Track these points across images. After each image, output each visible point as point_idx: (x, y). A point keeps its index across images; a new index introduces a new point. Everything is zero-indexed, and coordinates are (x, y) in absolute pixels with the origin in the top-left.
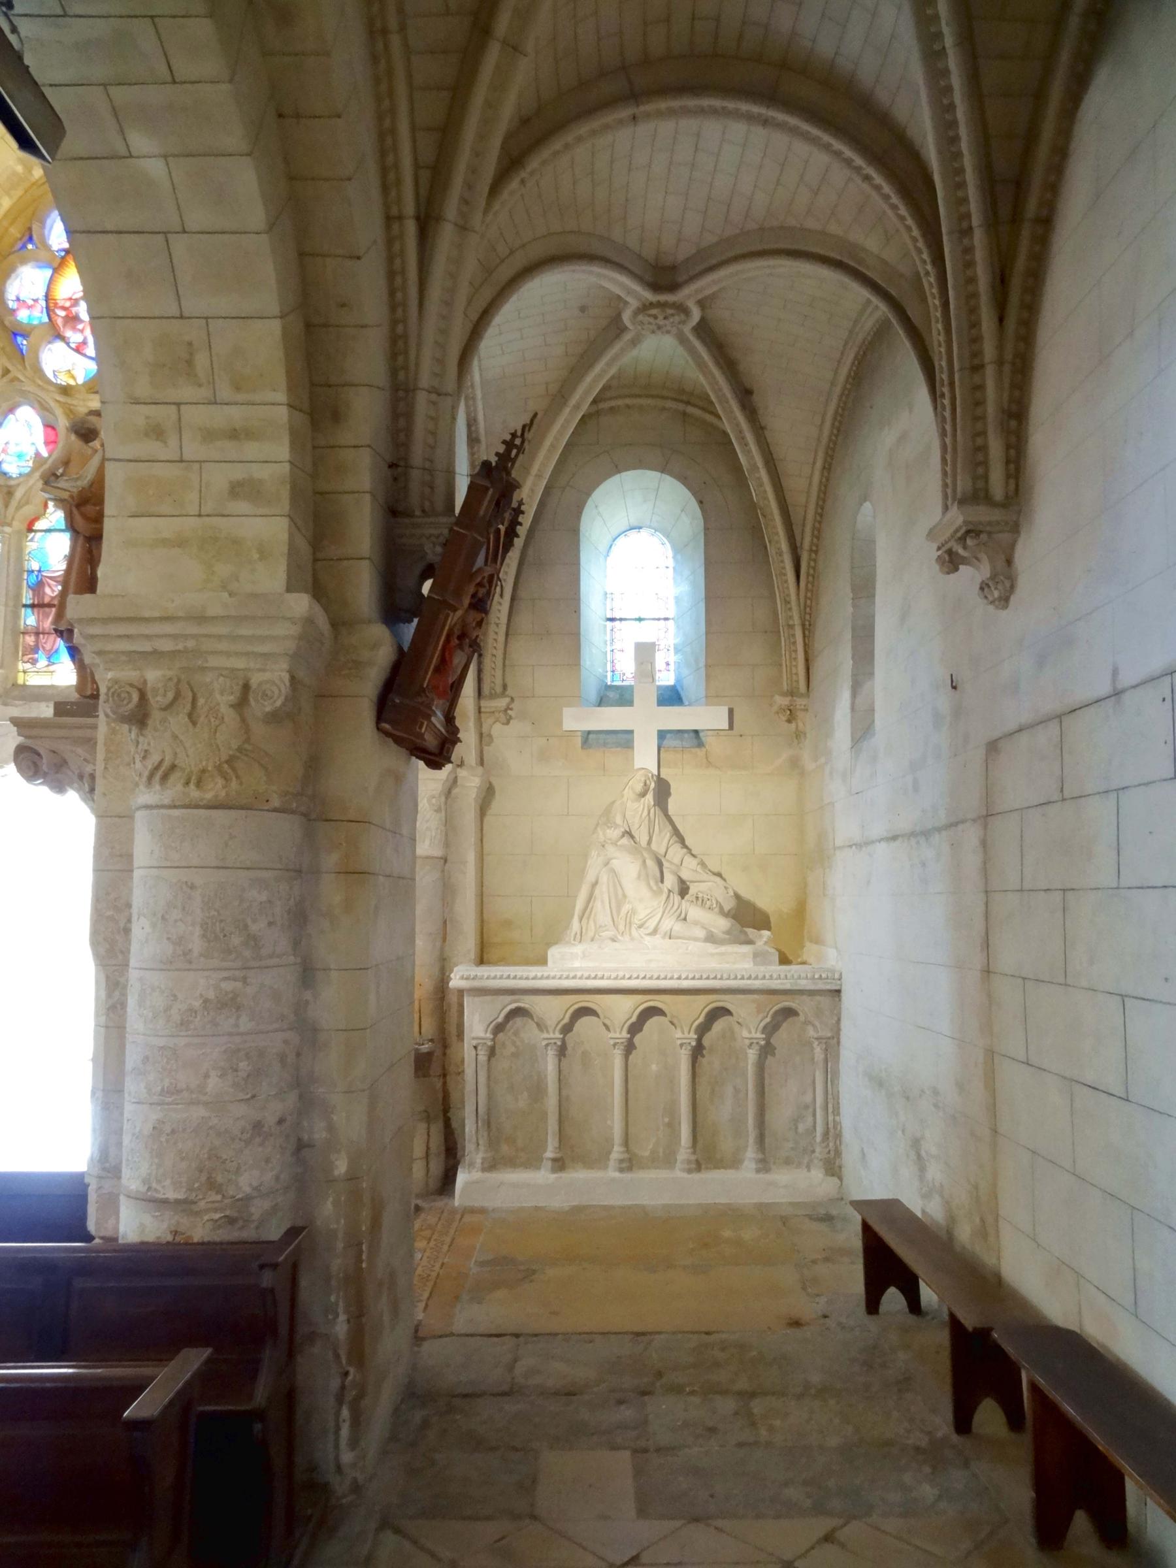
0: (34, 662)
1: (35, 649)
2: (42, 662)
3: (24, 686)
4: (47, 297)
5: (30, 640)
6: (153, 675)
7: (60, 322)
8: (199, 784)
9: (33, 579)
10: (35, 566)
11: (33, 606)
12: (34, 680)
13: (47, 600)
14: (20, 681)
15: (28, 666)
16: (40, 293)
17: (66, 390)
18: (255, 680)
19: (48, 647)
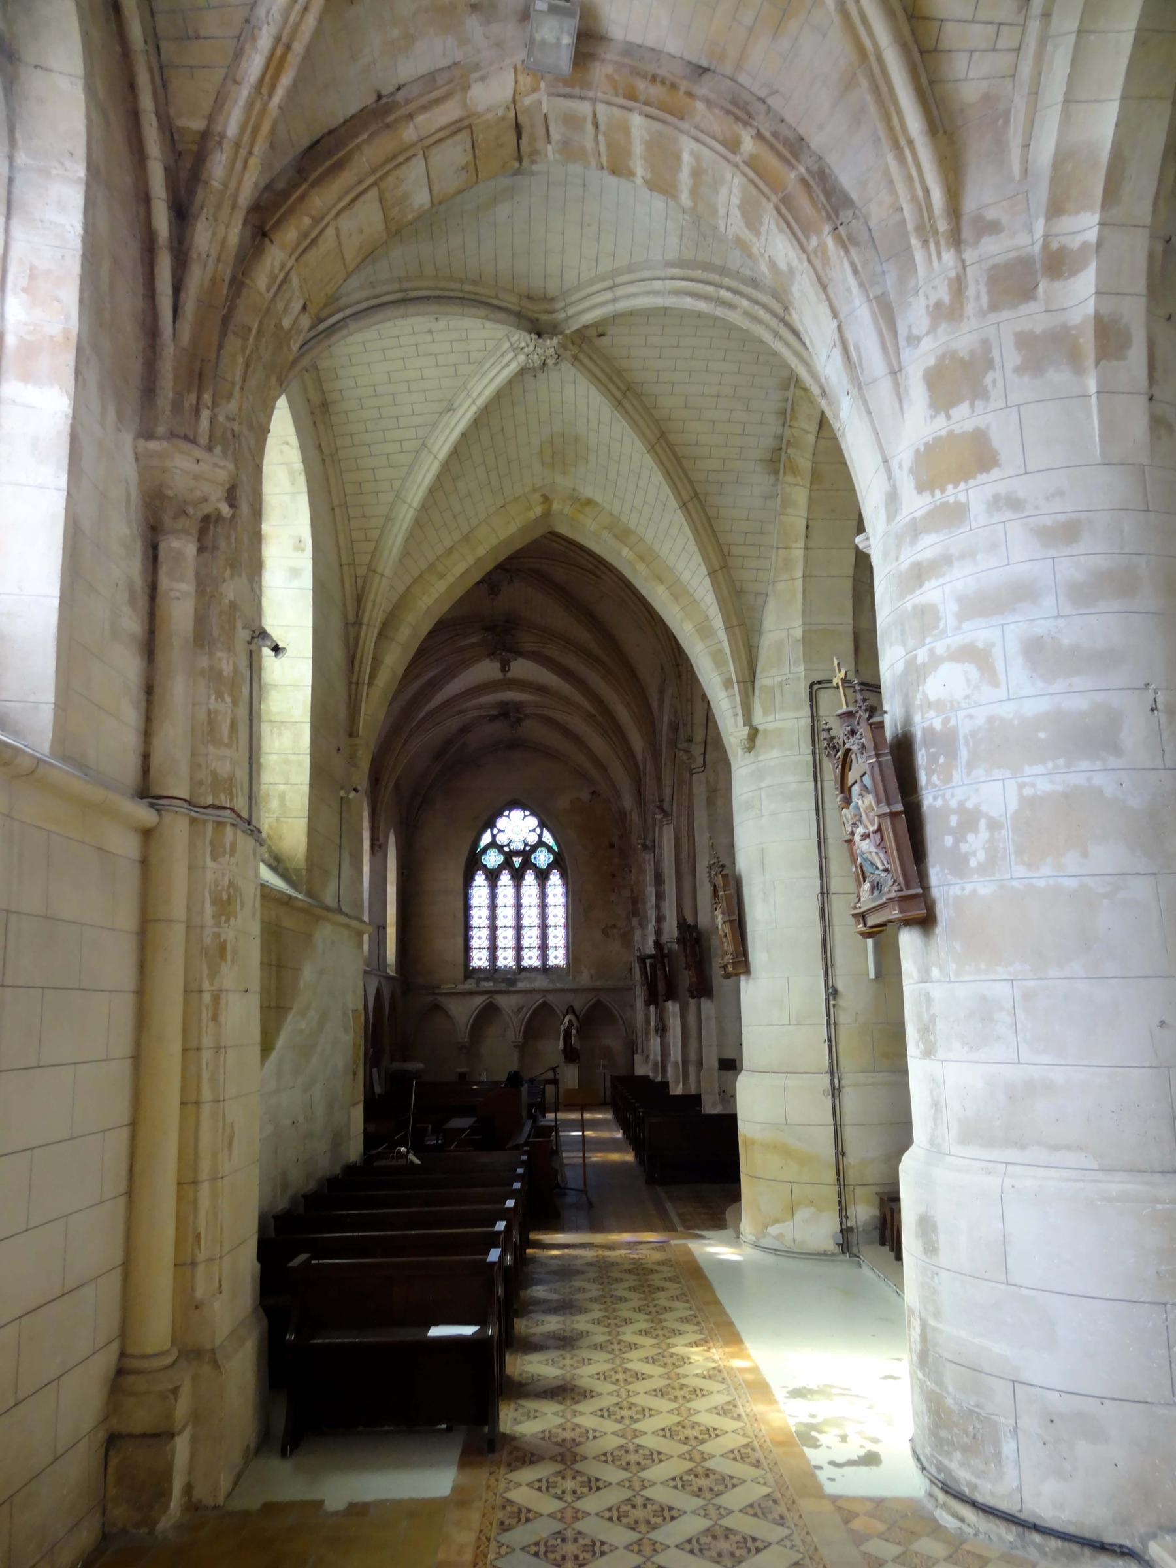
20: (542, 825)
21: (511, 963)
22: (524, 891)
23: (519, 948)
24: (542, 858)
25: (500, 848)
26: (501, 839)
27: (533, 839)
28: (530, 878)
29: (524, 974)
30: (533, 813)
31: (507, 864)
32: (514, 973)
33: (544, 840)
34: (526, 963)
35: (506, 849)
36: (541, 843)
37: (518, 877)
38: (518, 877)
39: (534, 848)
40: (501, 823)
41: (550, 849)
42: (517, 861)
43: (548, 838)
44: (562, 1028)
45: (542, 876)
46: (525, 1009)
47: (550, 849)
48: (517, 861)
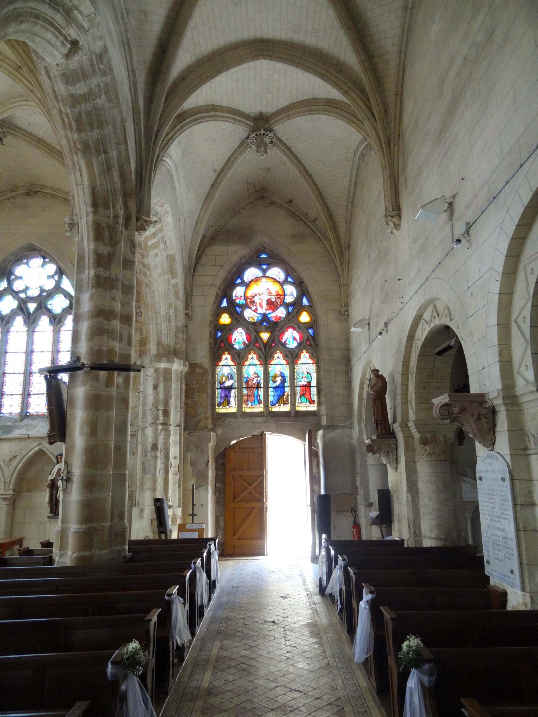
0: (247, 405)
1: (247, 401)
2: (250, 405)
3: (245, 412)
4: (245, 295)
5: (246, 398)
6: (428, 436)
7: (249, 303)
8: (438, 456)
9: (245, 380)
10: (246, 376)
11: (246, 388)
12: (248, 410)
13: (250, 386)
14: (243, 411)
15: (245, 406)
16: (242, 294)
17: (254, 324)
18: (448, 436)
19: (251, 400)
20: (60, 272)
21: (16, 410)
22: (37, 336)
23: (26, 395)
24: (58, 304)
25: (15, 294)
26: (18, 286)
27: (50, 285)
28: (44, 321)
29: (26, 421)
30: (53, 261)
31: (22, 309)
32: (16, 421)
33: (62, 286)
34: (32, 410)
35: (23, 295)
36: (58, 289)
37: (31, 321)
38: (31, 321)
39: (51, 294)
40: (20, 270)
41: (67, 295)
42: (32, 307)
43: (67, 284)
44: (50, 478)
45: (57, 321)
46: (18, 459)
47: (67, 295)
48: (32, 307)
